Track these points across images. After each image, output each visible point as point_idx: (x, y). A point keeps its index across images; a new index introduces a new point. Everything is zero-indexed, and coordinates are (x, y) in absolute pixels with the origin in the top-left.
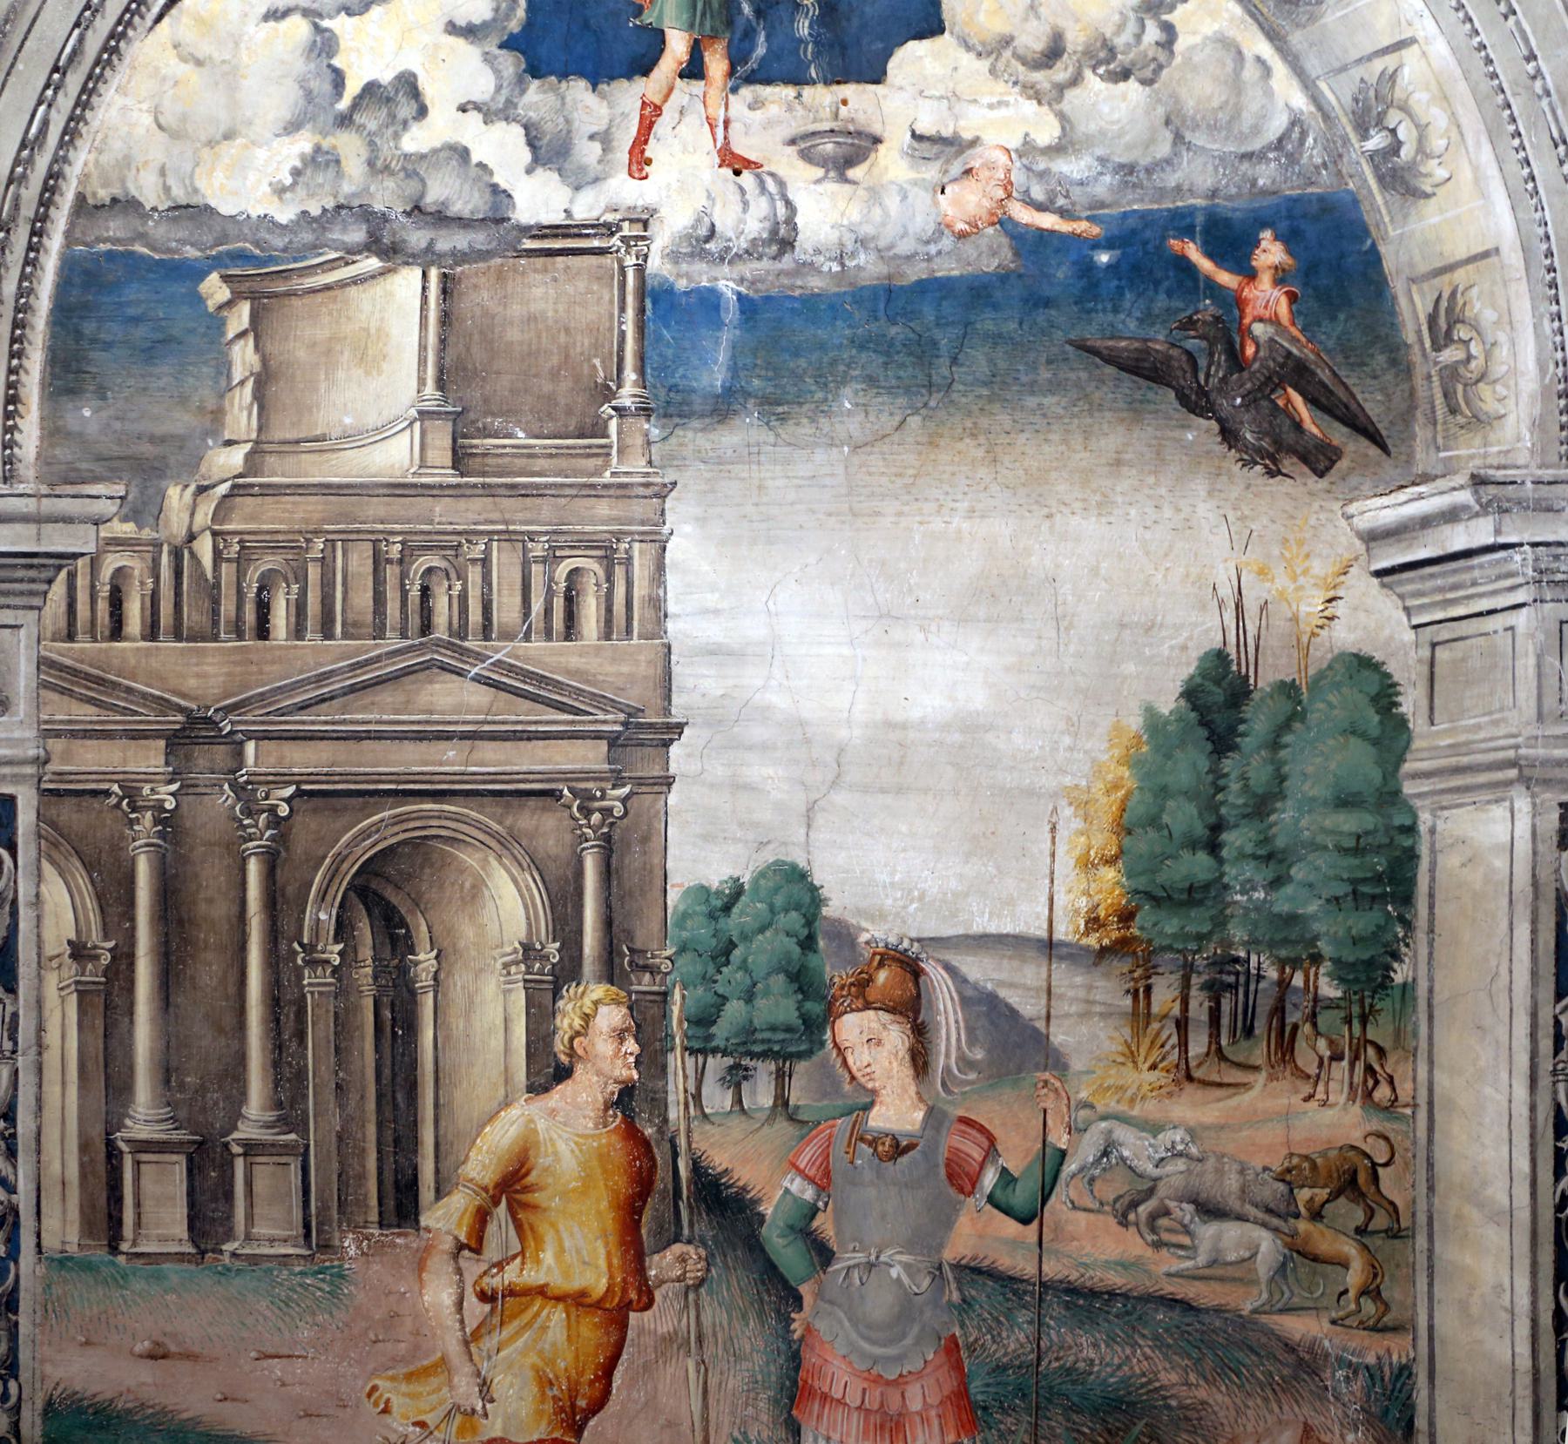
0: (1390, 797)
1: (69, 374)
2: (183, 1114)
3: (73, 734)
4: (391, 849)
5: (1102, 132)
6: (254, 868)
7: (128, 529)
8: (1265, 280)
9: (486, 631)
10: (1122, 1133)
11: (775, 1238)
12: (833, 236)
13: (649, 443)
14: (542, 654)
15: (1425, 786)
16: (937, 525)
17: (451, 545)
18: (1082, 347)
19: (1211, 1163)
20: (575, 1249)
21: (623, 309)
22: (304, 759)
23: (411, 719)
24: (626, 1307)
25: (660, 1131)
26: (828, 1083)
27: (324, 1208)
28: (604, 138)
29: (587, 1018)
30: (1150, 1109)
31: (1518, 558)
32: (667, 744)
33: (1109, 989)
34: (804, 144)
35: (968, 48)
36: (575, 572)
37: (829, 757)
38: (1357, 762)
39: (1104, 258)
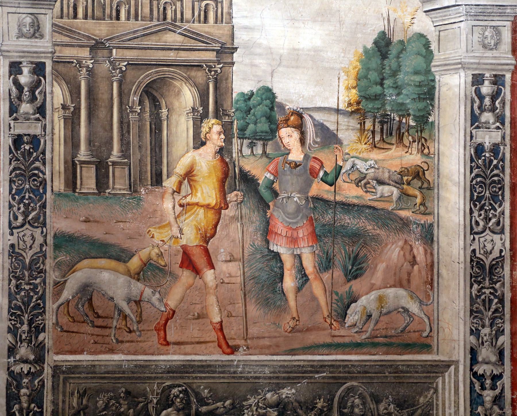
0: (428, 72)
2: (94, 153)
3: (63, 45)
4: (154, 81)
6: (115, 85)
9: (182, 20)
10: (357, 161)
11: (262, 190)
14: (197, 27)
15: (437, 69)
19: (381, 170)
20: (207, 192)
24: (221, 208)
25: (231, 160)
26: (277, 147)
27: (135, 181)
30: (365, 155)
31: (461, 8)
32: (233, 53)
33: (354, 122)
36: (207, 5)
37: (278, 58)
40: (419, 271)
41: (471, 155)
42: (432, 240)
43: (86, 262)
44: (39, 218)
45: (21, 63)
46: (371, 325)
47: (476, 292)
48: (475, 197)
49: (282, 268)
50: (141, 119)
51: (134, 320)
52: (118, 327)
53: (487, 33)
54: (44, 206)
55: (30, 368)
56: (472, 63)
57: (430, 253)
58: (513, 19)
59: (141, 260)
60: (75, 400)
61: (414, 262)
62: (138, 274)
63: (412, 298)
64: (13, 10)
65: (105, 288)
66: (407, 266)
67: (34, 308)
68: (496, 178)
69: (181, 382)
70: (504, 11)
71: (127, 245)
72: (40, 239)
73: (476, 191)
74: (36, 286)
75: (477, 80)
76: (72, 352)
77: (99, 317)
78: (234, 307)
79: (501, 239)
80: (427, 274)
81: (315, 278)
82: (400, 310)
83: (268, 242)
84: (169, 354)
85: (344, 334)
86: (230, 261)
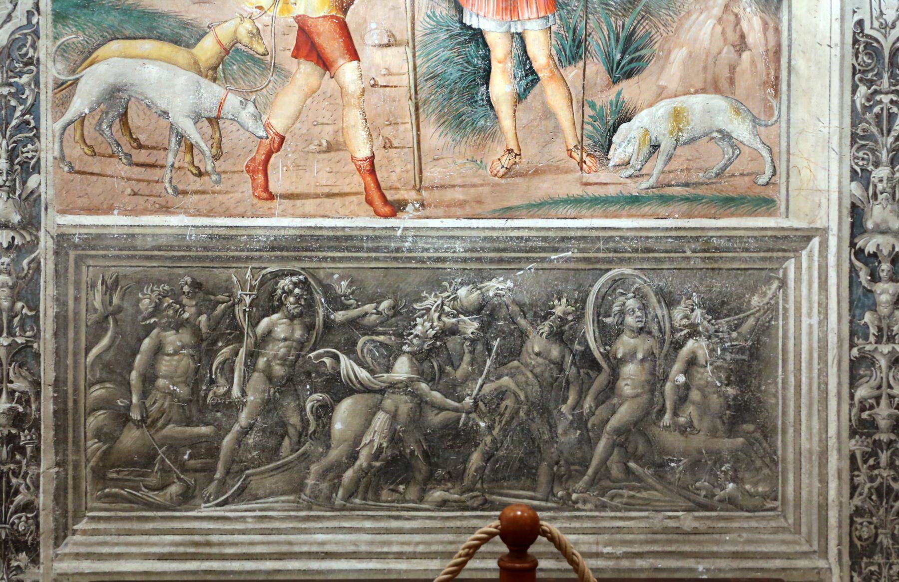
40: (753, 62)
43: (114, 45)
47: (863, 101)
51: (208, 153)
52: (176, 165)
55: (13, 238)
59: (219, 42)
60: (98, 297)
62: (215, 68)
63: (737, 112)
65: (151, 94)
67: (18, 128)
69: (296, 266)
71: (193, 16)
74: (20, 89)
76: (91, 210)
77: (140, 146)
78: (397, 131)
82: (715, 134)
84: (273, 215)
85: (608, 179)
86: (389, 45)
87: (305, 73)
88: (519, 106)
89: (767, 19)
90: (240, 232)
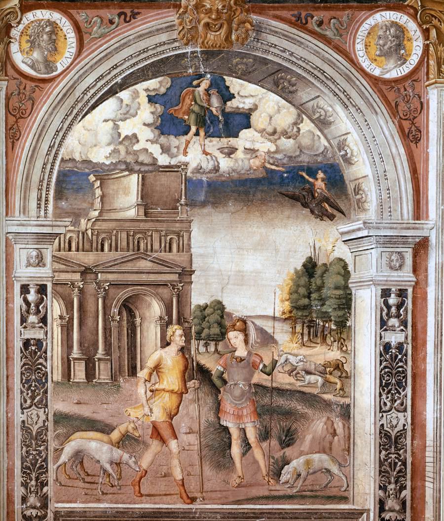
0: (346, 287)
1: (60, 194)
2: (84, 352)
3: (60, 272)
4: (130, 297)
5: (285, 149)
6: (100, 301)
7: (72, 228)
8: (320, 181)
9: (152, 250)
10: (289, 357)
12: (227, 169)
13: (187, 211)
15: (354, 285)
16: (250, 229)
17: (144, 232)
18: (281, 193)
19: (308, 363)
20: (171, 380)
21: (182, 183)
22: (111, 277)
23: (135, 269)
24: (182, 393)
25: (190, 356)
27: (116, 372)
28: (178, 147)
29: (174, 332)
30: (295, 351)
32: (191, 275)
33: (287, 327)
34: (221, 150)
35: (256, 131)
37: (227, 278)
38: (340, 280)
39: (285, 175)
40: (339, 441)
41: (381, 351)
42: (349, 417)
43: (78, 434)
44: (42, 401)
45: (28, 285)
46: (300, 482)
48: (384, 384)
49: (230, 438)
50: (120, 326)
51: (116, 478)
52: (103, 483)
53: (393, 258)
54: (46, 392)
56: (381, 281)
57: (347, 428)
58: (413, 246)
59: (120, 432)
61: (334, 434)
62: (118, 443)
64: (23, 246)
65: (93, 454)
66: (329, 437)
67: (40, 468)
68: (400, 369)
70: (406, 240)
71: (110, 421)
72: (43, 417)
73: (384, 379)
74: (40, 452)
75: (386, 293)
76: (68, 502)
77: (88, 475)
78: (193, 468)
79: (404, 416)
80: (345, 444)
81: (256, 447)
82: (324, 470)
83: (219, 419)
84: (142, 503)
85: (281, 489)
86: (189, 433)
87: (155, 445)
88: (243, 458)
89: (345, 423)
90: (129, 510)
